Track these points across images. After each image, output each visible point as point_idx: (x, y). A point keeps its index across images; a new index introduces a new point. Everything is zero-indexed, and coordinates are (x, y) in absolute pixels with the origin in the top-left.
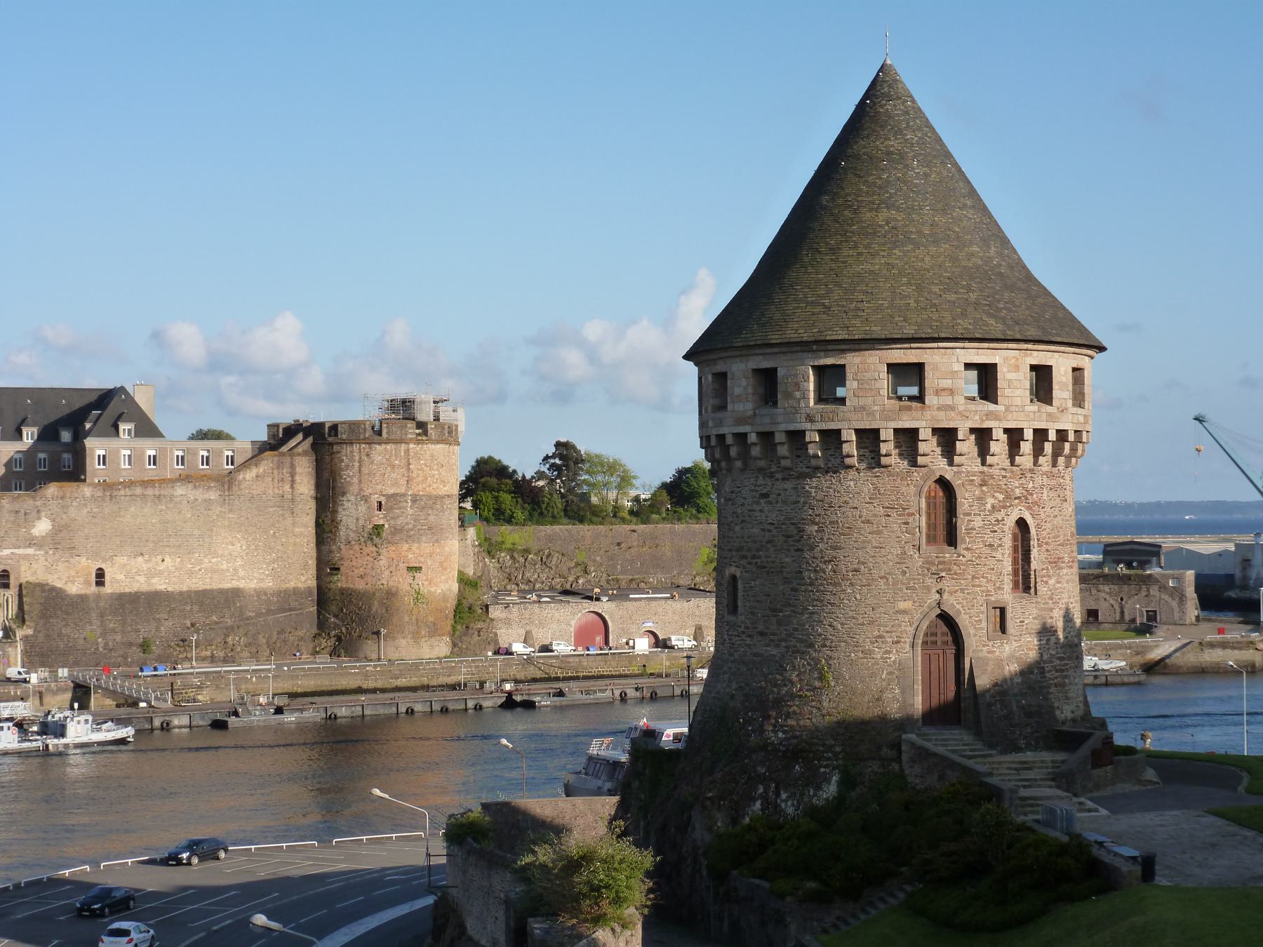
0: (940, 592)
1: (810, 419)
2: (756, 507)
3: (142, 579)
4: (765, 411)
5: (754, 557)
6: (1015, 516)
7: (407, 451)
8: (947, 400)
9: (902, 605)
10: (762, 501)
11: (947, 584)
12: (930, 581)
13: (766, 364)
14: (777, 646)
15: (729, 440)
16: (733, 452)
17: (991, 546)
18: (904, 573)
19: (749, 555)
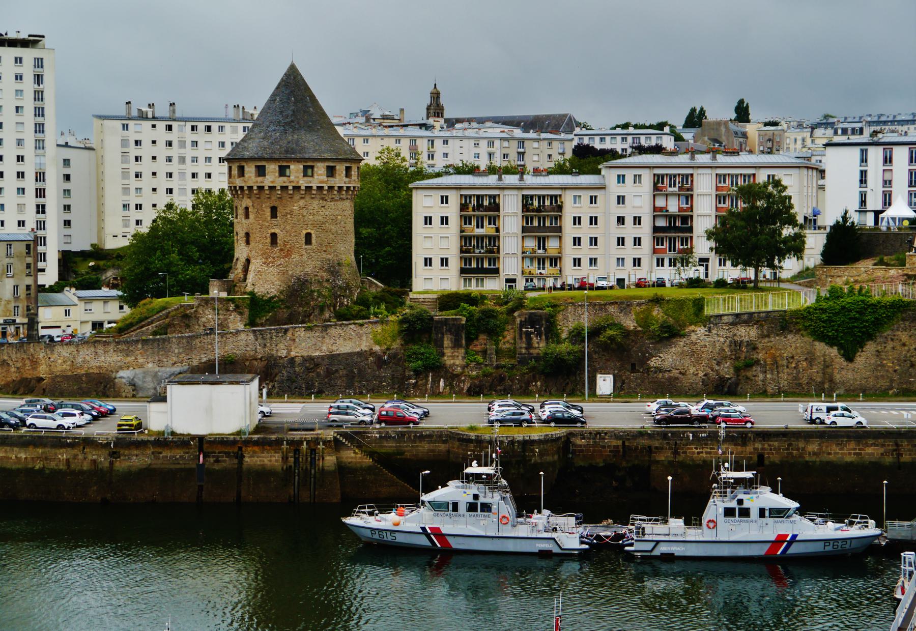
1: (345, 183)
4: (330, 179)
13: (332, 164)
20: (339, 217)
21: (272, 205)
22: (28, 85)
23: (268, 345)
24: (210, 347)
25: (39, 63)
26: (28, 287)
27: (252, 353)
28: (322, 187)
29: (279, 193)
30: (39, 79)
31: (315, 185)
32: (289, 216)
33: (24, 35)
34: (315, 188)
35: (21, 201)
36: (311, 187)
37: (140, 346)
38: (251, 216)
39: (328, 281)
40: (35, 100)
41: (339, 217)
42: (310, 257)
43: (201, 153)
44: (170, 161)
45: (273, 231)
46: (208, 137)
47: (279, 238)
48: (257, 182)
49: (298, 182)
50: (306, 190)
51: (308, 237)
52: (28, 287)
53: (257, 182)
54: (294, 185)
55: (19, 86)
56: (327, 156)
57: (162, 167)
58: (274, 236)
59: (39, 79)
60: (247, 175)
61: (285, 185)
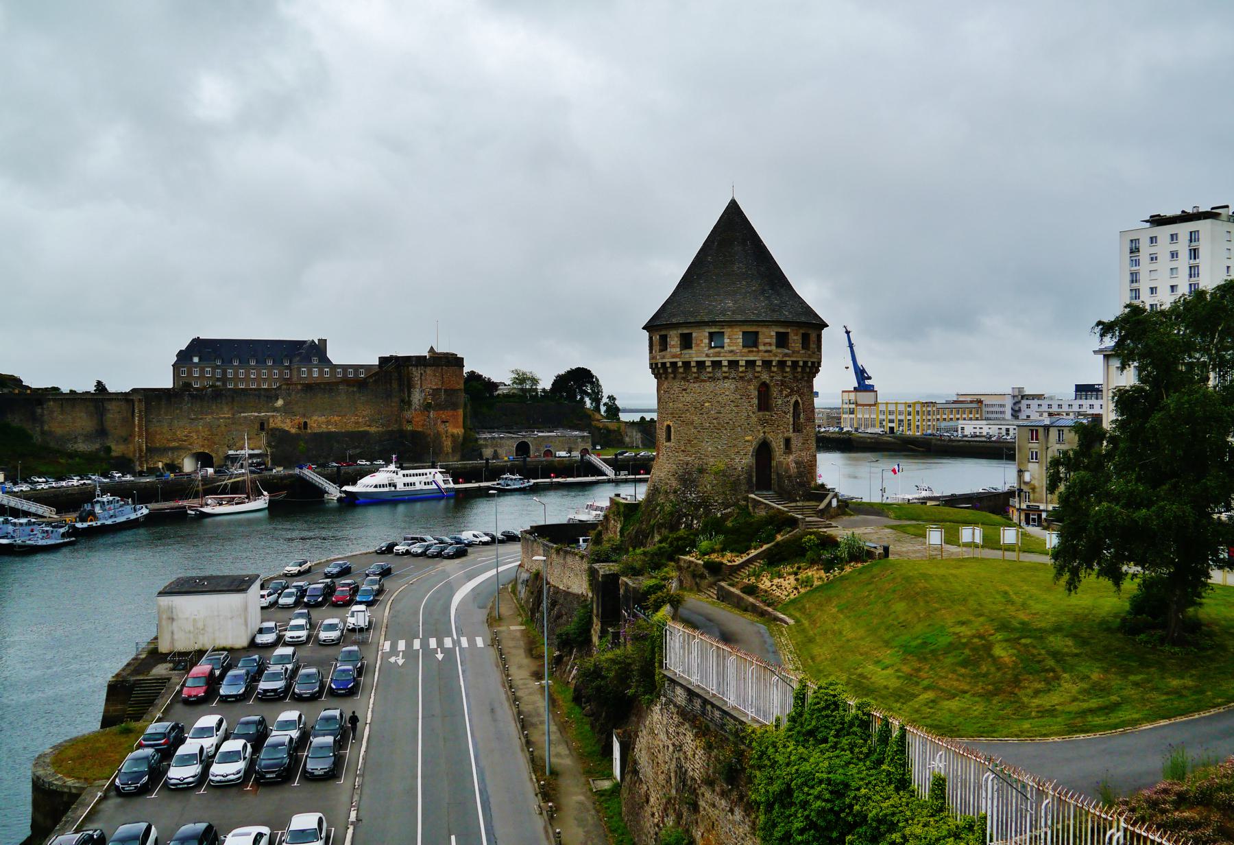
0: (764, 433)
1: (707, 356)
3: (324, 426)
6: (794, 400)
7: (442, 369)
8: (768, 348)
9: (747, 438)
11: (766, 429)
12: (759, 428)
13: (686, 331)
14: (691, 457)
15: (668, 365)
17: (785, 412)
18: (748, 424)
20: (707, 404)
22: (1184, 261)
28: (676, 363)
30: (1194, 253)
31: (668, 360)
39: (675, 492)
40: (1191, 277)
42: (669, 458)
50: (746, 366)
55: (1174, 265)
56: (674, 321)
59: (1194, 253)
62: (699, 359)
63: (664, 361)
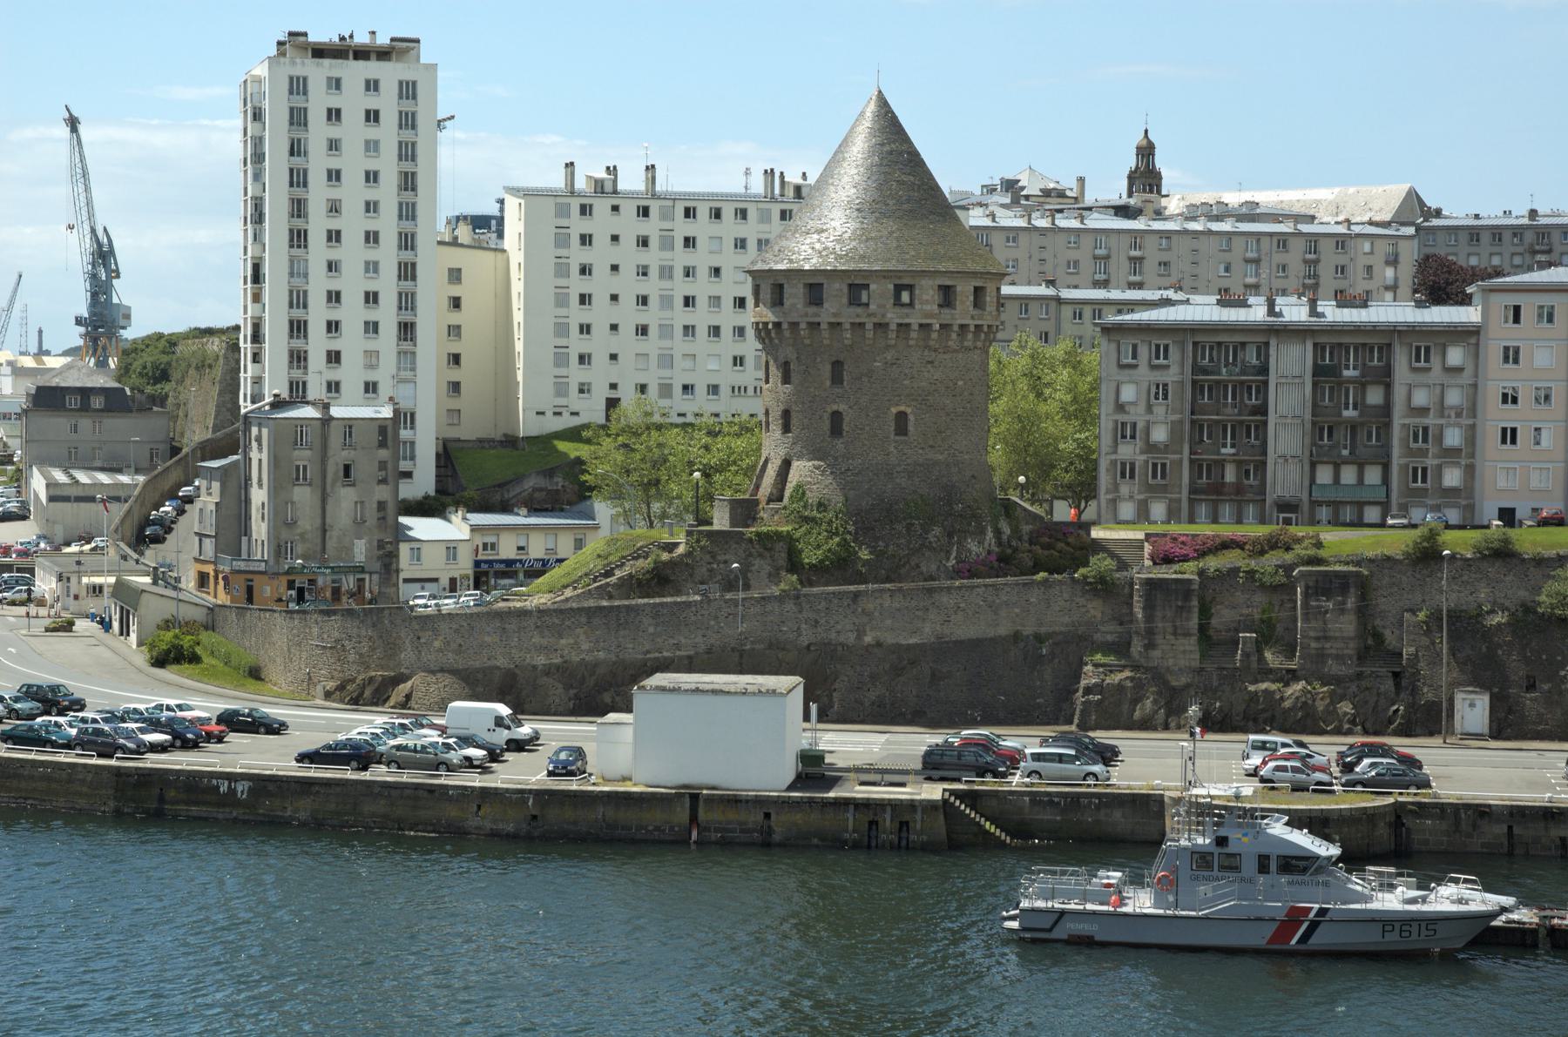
1: (973, 318)
2: (923, 369)
4: (946, 311)
5: (924, 400)
10: (929, 366)
13: (948, 283)
16: (914, 335)
19: (920, 398)
20: (960, 383)
21: (834, 359)
23: (823, 621)
24: (712, 623)
25: (408, 90)
26: (381, 506)
27: (792, 636)
28: (929, 325)
29: (848, 336)
31: (914, 321)
32: (865, 379)
33: (383, 40)
34: (916, 327)
35: (372, 345)
36: (908, 325)
37: (583, 620)
38: (795, 377)
41: (960, 383)
43: (701, 259)
44: (645, 274)
45: (835, 407)
46: (716, 228)
47: (847, 419)
48: (806, 315)
49: (883, 316)
51: (902, 417)
52: (381, 506)
53: (806, 315)
54: (876, 320)
57: (629, 285)
58: (836, 417)
60: (787, 303)
61: (858, 320)
62: (964, 322)
63: (907, 321)
